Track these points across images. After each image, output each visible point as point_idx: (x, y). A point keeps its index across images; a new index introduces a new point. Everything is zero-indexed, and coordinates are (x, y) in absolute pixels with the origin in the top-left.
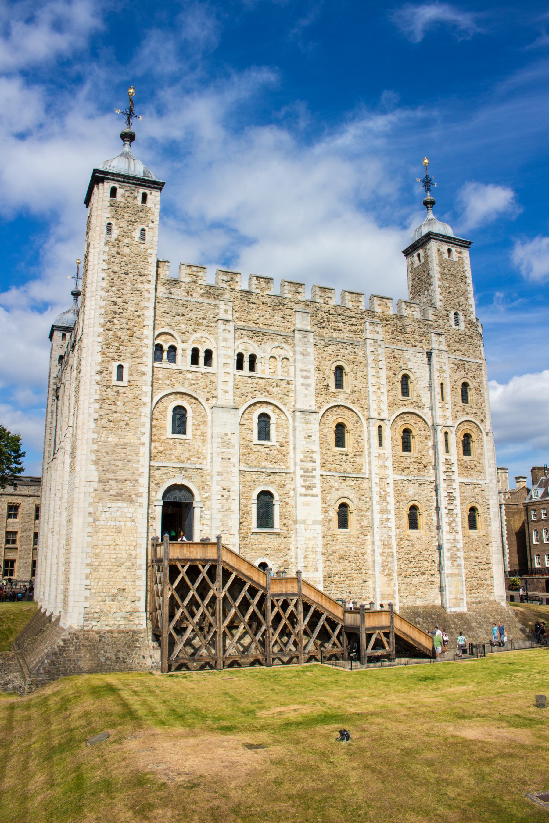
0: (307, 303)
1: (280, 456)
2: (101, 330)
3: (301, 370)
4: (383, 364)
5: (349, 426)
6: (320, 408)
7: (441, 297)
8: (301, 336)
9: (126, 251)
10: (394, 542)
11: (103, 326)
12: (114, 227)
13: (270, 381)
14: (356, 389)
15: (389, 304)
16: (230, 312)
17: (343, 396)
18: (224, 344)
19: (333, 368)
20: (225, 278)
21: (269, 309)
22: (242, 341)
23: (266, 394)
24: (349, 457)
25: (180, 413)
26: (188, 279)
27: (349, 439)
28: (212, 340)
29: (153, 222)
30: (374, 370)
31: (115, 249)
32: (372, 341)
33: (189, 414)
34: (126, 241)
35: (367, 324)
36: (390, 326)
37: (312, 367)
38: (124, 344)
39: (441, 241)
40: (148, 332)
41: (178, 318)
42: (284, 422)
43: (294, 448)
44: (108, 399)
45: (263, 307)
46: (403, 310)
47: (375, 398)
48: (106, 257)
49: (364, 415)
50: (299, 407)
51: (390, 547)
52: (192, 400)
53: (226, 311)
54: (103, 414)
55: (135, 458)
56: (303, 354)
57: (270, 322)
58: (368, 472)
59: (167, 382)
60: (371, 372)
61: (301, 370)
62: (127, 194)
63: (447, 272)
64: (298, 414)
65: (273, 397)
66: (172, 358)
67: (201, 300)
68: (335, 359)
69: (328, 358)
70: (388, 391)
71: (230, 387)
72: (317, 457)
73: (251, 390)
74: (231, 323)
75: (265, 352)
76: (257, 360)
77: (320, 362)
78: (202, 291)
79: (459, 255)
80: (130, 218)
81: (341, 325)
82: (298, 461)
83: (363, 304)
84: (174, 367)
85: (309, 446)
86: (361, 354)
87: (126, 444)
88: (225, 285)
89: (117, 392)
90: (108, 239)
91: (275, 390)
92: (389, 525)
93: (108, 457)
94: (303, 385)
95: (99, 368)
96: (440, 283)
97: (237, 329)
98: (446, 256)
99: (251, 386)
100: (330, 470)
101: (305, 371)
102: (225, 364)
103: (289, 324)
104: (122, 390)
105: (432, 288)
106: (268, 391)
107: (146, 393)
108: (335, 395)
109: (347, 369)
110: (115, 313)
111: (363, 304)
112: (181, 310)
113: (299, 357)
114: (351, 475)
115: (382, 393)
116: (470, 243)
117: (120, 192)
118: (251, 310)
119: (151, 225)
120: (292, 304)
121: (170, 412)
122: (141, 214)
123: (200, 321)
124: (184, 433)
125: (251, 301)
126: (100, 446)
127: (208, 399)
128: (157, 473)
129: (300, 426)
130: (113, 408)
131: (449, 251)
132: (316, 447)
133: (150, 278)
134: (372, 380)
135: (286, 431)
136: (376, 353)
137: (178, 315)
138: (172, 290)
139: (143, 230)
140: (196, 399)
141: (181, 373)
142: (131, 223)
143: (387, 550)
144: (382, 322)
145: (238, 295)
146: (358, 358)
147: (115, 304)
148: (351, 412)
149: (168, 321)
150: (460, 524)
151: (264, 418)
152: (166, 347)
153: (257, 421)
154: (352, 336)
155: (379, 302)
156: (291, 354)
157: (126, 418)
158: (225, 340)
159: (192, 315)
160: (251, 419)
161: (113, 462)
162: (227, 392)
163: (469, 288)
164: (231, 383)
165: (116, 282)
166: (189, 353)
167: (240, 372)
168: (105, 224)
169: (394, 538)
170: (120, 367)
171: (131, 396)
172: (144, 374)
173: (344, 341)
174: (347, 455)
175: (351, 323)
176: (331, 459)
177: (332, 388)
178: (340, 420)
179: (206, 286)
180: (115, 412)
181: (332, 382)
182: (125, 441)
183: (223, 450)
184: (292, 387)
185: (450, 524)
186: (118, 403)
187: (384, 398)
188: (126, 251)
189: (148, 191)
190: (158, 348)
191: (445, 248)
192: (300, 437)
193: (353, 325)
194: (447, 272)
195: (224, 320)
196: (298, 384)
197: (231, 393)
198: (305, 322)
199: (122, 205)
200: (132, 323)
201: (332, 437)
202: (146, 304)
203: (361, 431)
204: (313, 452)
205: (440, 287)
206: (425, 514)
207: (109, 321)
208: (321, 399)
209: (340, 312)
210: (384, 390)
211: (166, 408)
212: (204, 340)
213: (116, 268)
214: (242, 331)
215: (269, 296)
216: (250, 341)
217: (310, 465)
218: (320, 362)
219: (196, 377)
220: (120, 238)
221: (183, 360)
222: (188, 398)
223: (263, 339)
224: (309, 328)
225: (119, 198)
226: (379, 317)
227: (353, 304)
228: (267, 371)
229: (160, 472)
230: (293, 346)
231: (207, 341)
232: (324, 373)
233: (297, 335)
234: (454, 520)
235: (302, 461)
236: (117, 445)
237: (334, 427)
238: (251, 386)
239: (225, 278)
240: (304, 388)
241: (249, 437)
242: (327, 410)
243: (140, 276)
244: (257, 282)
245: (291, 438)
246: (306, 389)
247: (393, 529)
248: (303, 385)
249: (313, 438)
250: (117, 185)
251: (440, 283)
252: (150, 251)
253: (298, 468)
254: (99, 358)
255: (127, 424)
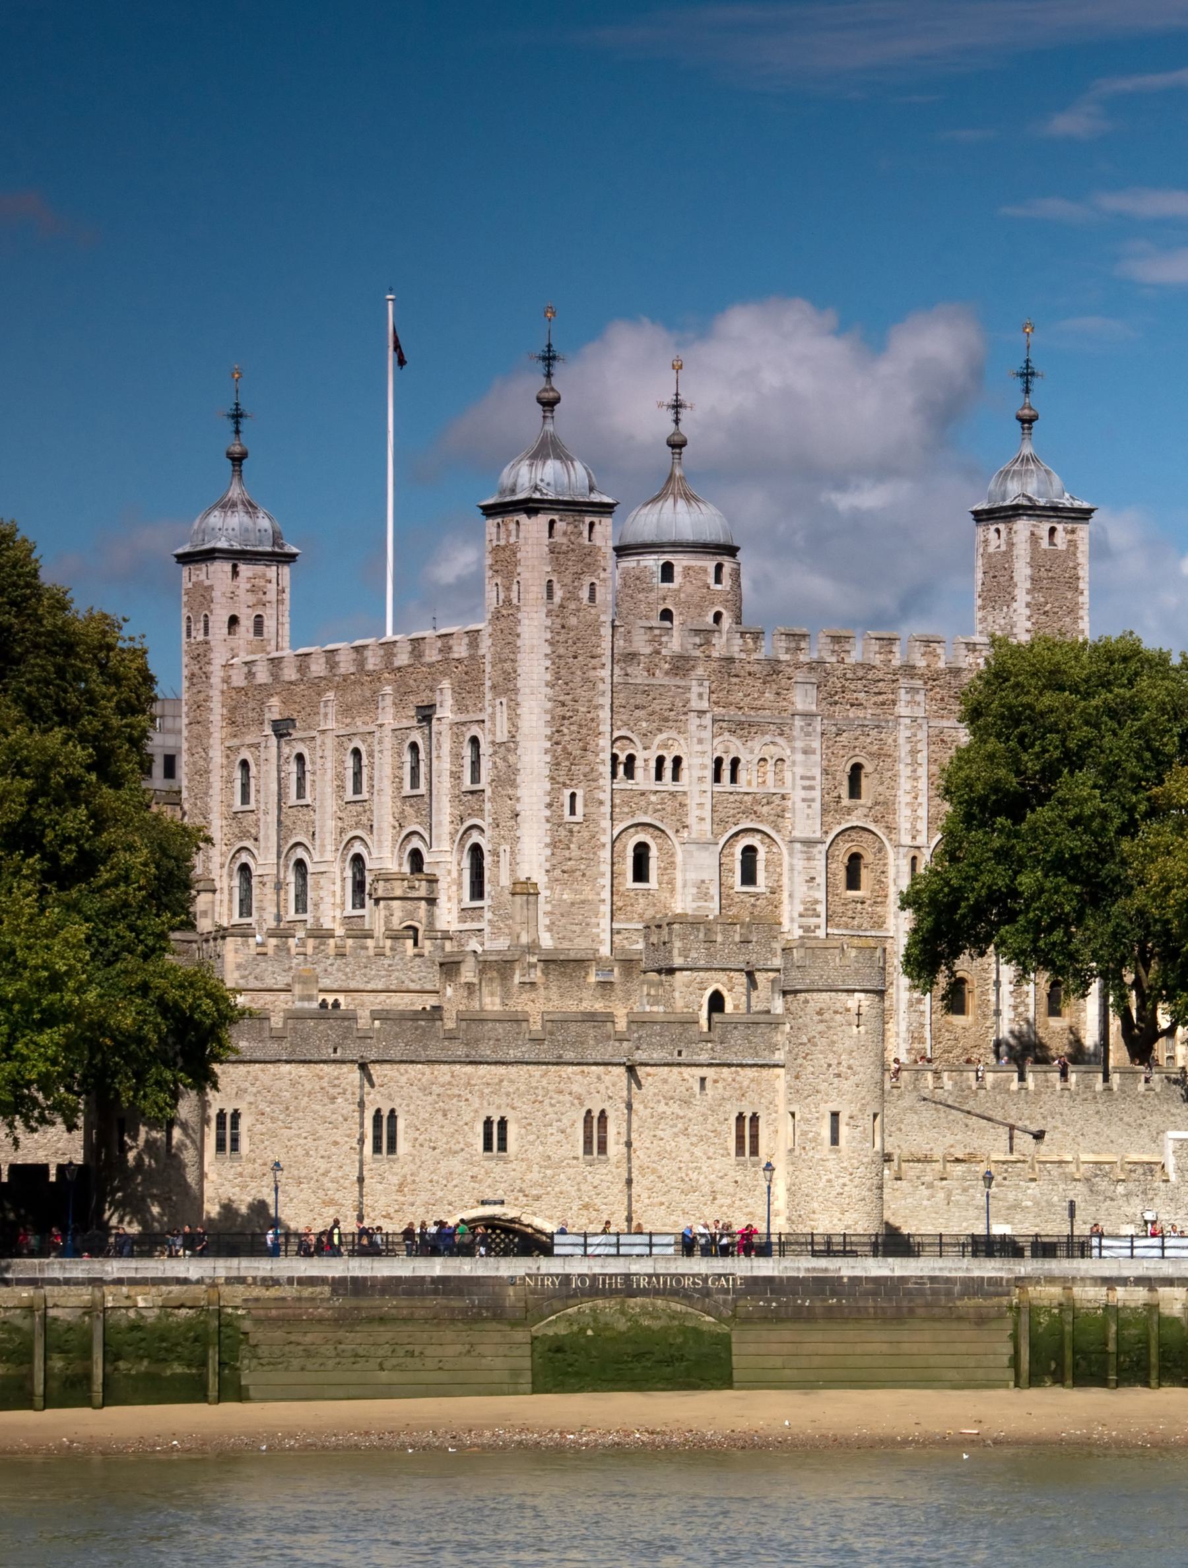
0: (812, 667)
1: (770, 908)
2: (548, 745)
3: (802, 778)
4: (922, 757)
5: (868, 857)
6: (826, 832)
7: (1029, 625)
8: (802, 724)
9: (573, 621)
10: (927, 1035)
11: (550, 740)
12: (556, 586)
13: (758, 797)
14: (881, 798)
15: (939, 651)
16: (706, 697)
17: (860, 812)
18: (699, 748)
19: (848, 769)
20: (697, 640)
21: (758, 684)
22: (720, 739)
23: (753, 816)
24: (866, 906)
25: (641, 854)
26: (648, 650)
27: (865, 875)
28: (682, 742)
29: (605, 570)
30: (910, 768)
31: (558, 621)
32: (908, 721)
33: (654, 853)
34: (573, 606)
35: (903, 691)
36: (938, 690)
37: (817, 772)
38: (576, 762)
39: (1038, 516)
40: (604, 742)
41: (638, 713)
42: (776, 857)
43: (790, 896)
44: (560, 841)
45: (749, 680)
46: (961, 659)
47: (908, 812)
48: (549, 636)
49: (891, 840)
50: (797, 834)
51: (921, 1040)
52: (657, 833)
53: (700, 695)
54: (555, 862)
55: (594, 920)
56: (805, 752)
57: (758, 703)
58: (892, 928)
59: (626, 810)
60: (904, 771)
61: (802, 778)
62: (570, 528)
63: (1043, 574)
64: (798, 846)
65: (761, 821)
66: (630, 773)
67: (666, 681)
68: (852, 753)
69: (841, 752)
70: (929, 798)
71: (707, 814)
72: (821, 909)
73: (732, 812)
74: (709, 715)
75: (752, 752)
76: (740, 766)
77: (829, 761)
78: (667, 666)
79: (1069, 537)
80: (575, 569)
81: (863, 694)
82: (796, 915)
83: (898, 655)
84: (635, 787)
85: (811, 893)
86: (890, 741)
87: (583, 902)
88: (697, 653)
89: (571, 831)
90: (550, 607)
91: (765, 810)
92: (922, 1008)
93: (564, 921)
94: (804, 800)
95: (548, 799)
96: (1028, 598)
97: (714, 721)
98: (1045, 544)
99: (733, 806)
100: (838, 926)
101: (808, 778)
102: (701, 779)
103: (785, 704)
104: (576, 828)
105: (1015, 605)
106: (755, 812)
107: (604, 830)
108: (849, 811)
109: (868, 767)
110: (564, 718)
111: (898, 655)
112: (640, 699)
113: (799, 757)
114: (868, 934)
115: (920, 804)
116: (1092, 510)
117: (560, 526)
118: (733, 687)
119: (602, 575)
120: (790, 670)
121: (630, 853)
122: (588, 560)
123: (666, 714)
124: (648, 881)
125: (733, 672)
126: (554, 906)
127: (677, 831)
128: (616, 938)
129: (800, 864)
130: (566, 853)
131: (1052, 531)
132: (821, 895)
133: (604, 660)
134: (905, 784)
135: (778, 870)
136: (914, 739)
137: (637, 707)
138: (629, 670)
139: (593, 584)
140: (663, 831)
141: (643, 794)
142: (578, 576)
143: (916, 1046)
144: (926, 683)
145: (715, 665)
146: (886, 748)
147: (564, 705)
148: (872, 836)
149: (624, 717)
150: (1032, 1008)
151: (750, 851)
152: (622, 758)
153: (740, 857)
154: (879, 711)
155: (923, 649)
156: (788, 752)
157: (583, 867)
158: (700, 741)
159: (656, 706)
160: (733, 855)
161: (569, 927)
162: (703, 819)
163: (1081, 599)
164: (708, 807)
165: (563, 672)
166: (653, 764)
167: (718, 788)
168: (545, 583)
169: (928, 1027)
170: (573, 796)
171: (586, 834)
172: (601, 803)
173: (867, 723)
174: (863, 903)
175: (876, 690)
176: (840, 910)
177: (846, 801)
178: (854, 850)
179: (672, 657)
180: (570, 859)
181: (844, 791)
182: (582, 897)
183: (700, 904)
184: (789, 803)
185: (1015, 1008)
186: (572, 846)
187: (923, 812)
188: (573, 621)
189: (596, 520)
190: (614, 757)
191: (1045, 526)
192: (800, 879)
193: (880, 693)
194: (1043, 574)
195: (699, 712)
196: (798, 800)
197: (709, 820)
198: (809, 700)
199: (564, 548)
200: (584, 731)
201: (842, 875)
202: (601, 700)
203: (885, 865)
204: (817, 902)
205: (1028, 605)
206: (977, 991)
207: (558, 731)
208: (829, 819)
209: (860, 673)
210: (923, 799)
211: (625, 847)
212: (670, 742)
213: (562, 651)
214: (721, 723)
215: (758, 661)
216: (733, 739)
217: (813, 921)
218: (829, 761)
219: (662, 799)
220: (565, 604)
221: (644, 778)
222: (651, 830)
223: (749, 733)
224: (814, 708)
225: (558, 538)
226: (922, 675)
227: (882, 657)
228: (754, 783)
229: (620, 937)
230: (790, 739)
231: (676, 744)
232: (834, 779)
233: (798, 722)
234: (1023, 1002)
235: (801, 916)
236: (573, 904)
237: (846, 860)
238: (733, 806)
239: (697, 640)
240: (805, 804)
241: (730, 881)
242: (837, 835)
243: (592, 657)
244: (741, 641)
245: (785, 880)
246: (809, 807)
247: (928, 1014)
248: (804, 800)
249: (818, 880)
250: (556, 517)
251: (1028, 598)
252: (603, 618)
253: (796, 925)
254: (548, 786)
255: (584, 875)
